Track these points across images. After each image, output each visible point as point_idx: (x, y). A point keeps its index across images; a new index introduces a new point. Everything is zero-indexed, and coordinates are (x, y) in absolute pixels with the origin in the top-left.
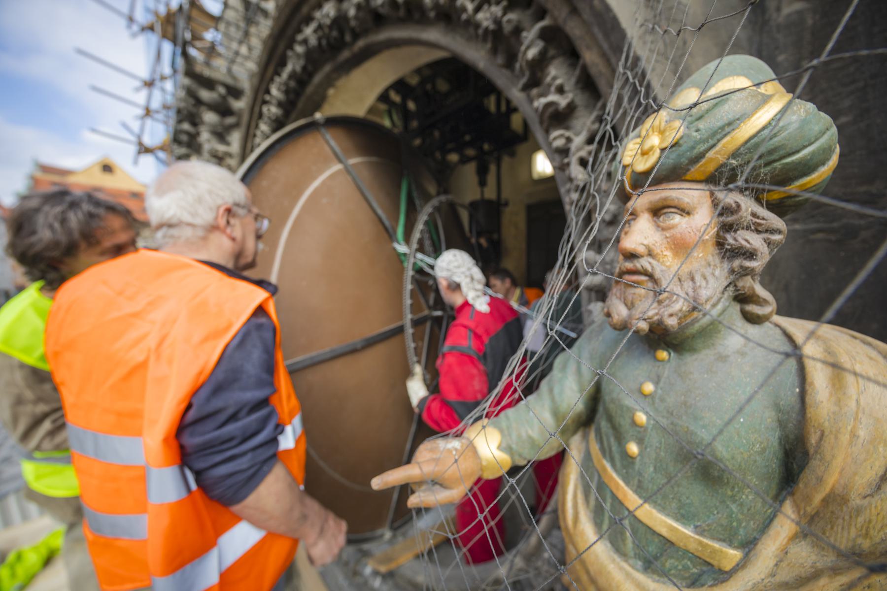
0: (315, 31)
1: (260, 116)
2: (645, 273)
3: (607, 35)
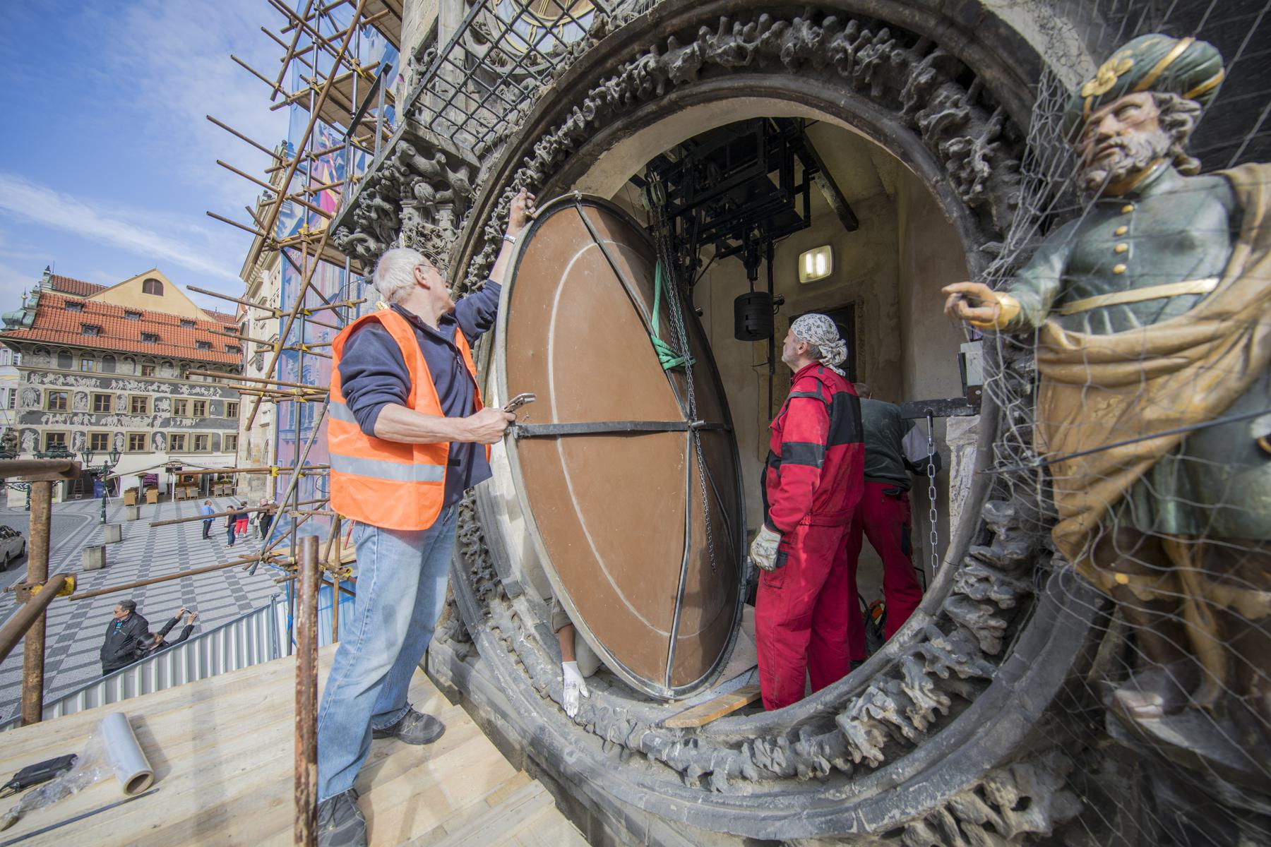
0: (618, 85)
1: (510, 181)
2: (1117, 145)
3: (1012, 53)
